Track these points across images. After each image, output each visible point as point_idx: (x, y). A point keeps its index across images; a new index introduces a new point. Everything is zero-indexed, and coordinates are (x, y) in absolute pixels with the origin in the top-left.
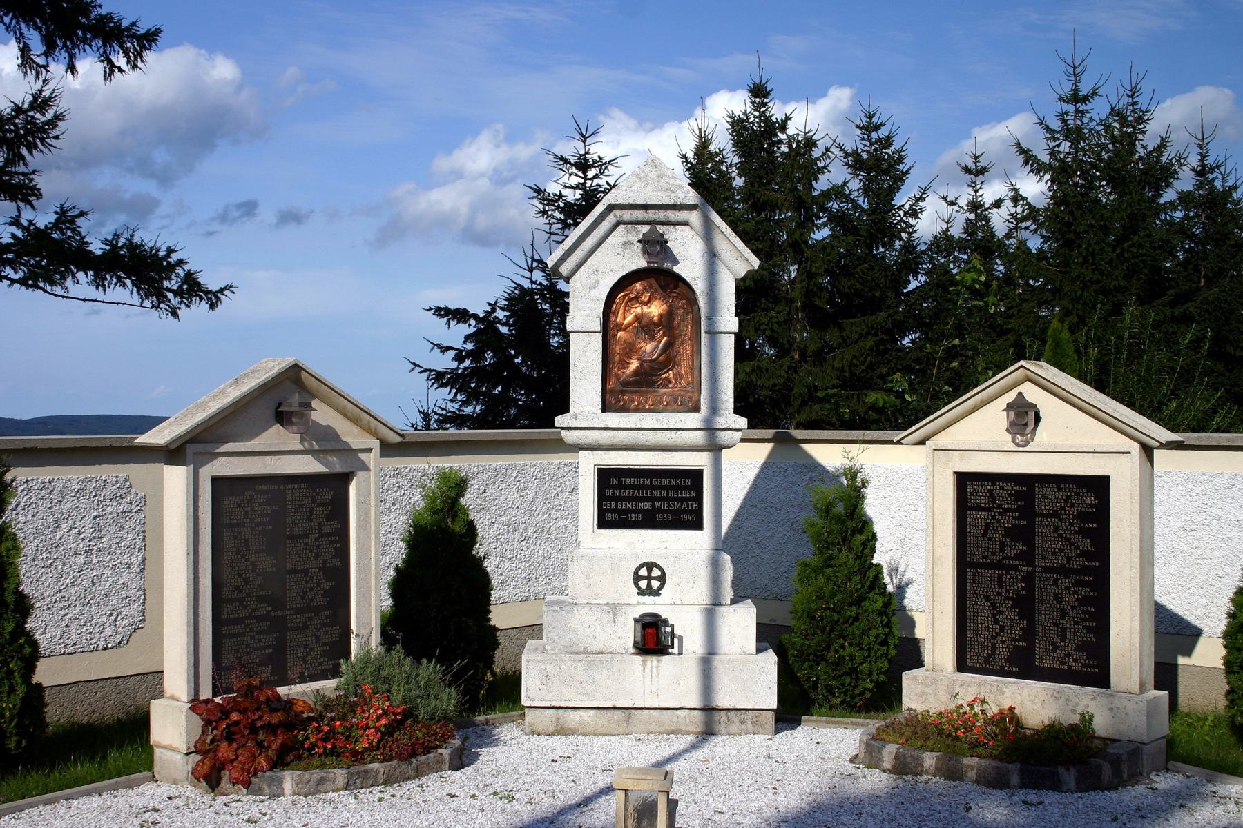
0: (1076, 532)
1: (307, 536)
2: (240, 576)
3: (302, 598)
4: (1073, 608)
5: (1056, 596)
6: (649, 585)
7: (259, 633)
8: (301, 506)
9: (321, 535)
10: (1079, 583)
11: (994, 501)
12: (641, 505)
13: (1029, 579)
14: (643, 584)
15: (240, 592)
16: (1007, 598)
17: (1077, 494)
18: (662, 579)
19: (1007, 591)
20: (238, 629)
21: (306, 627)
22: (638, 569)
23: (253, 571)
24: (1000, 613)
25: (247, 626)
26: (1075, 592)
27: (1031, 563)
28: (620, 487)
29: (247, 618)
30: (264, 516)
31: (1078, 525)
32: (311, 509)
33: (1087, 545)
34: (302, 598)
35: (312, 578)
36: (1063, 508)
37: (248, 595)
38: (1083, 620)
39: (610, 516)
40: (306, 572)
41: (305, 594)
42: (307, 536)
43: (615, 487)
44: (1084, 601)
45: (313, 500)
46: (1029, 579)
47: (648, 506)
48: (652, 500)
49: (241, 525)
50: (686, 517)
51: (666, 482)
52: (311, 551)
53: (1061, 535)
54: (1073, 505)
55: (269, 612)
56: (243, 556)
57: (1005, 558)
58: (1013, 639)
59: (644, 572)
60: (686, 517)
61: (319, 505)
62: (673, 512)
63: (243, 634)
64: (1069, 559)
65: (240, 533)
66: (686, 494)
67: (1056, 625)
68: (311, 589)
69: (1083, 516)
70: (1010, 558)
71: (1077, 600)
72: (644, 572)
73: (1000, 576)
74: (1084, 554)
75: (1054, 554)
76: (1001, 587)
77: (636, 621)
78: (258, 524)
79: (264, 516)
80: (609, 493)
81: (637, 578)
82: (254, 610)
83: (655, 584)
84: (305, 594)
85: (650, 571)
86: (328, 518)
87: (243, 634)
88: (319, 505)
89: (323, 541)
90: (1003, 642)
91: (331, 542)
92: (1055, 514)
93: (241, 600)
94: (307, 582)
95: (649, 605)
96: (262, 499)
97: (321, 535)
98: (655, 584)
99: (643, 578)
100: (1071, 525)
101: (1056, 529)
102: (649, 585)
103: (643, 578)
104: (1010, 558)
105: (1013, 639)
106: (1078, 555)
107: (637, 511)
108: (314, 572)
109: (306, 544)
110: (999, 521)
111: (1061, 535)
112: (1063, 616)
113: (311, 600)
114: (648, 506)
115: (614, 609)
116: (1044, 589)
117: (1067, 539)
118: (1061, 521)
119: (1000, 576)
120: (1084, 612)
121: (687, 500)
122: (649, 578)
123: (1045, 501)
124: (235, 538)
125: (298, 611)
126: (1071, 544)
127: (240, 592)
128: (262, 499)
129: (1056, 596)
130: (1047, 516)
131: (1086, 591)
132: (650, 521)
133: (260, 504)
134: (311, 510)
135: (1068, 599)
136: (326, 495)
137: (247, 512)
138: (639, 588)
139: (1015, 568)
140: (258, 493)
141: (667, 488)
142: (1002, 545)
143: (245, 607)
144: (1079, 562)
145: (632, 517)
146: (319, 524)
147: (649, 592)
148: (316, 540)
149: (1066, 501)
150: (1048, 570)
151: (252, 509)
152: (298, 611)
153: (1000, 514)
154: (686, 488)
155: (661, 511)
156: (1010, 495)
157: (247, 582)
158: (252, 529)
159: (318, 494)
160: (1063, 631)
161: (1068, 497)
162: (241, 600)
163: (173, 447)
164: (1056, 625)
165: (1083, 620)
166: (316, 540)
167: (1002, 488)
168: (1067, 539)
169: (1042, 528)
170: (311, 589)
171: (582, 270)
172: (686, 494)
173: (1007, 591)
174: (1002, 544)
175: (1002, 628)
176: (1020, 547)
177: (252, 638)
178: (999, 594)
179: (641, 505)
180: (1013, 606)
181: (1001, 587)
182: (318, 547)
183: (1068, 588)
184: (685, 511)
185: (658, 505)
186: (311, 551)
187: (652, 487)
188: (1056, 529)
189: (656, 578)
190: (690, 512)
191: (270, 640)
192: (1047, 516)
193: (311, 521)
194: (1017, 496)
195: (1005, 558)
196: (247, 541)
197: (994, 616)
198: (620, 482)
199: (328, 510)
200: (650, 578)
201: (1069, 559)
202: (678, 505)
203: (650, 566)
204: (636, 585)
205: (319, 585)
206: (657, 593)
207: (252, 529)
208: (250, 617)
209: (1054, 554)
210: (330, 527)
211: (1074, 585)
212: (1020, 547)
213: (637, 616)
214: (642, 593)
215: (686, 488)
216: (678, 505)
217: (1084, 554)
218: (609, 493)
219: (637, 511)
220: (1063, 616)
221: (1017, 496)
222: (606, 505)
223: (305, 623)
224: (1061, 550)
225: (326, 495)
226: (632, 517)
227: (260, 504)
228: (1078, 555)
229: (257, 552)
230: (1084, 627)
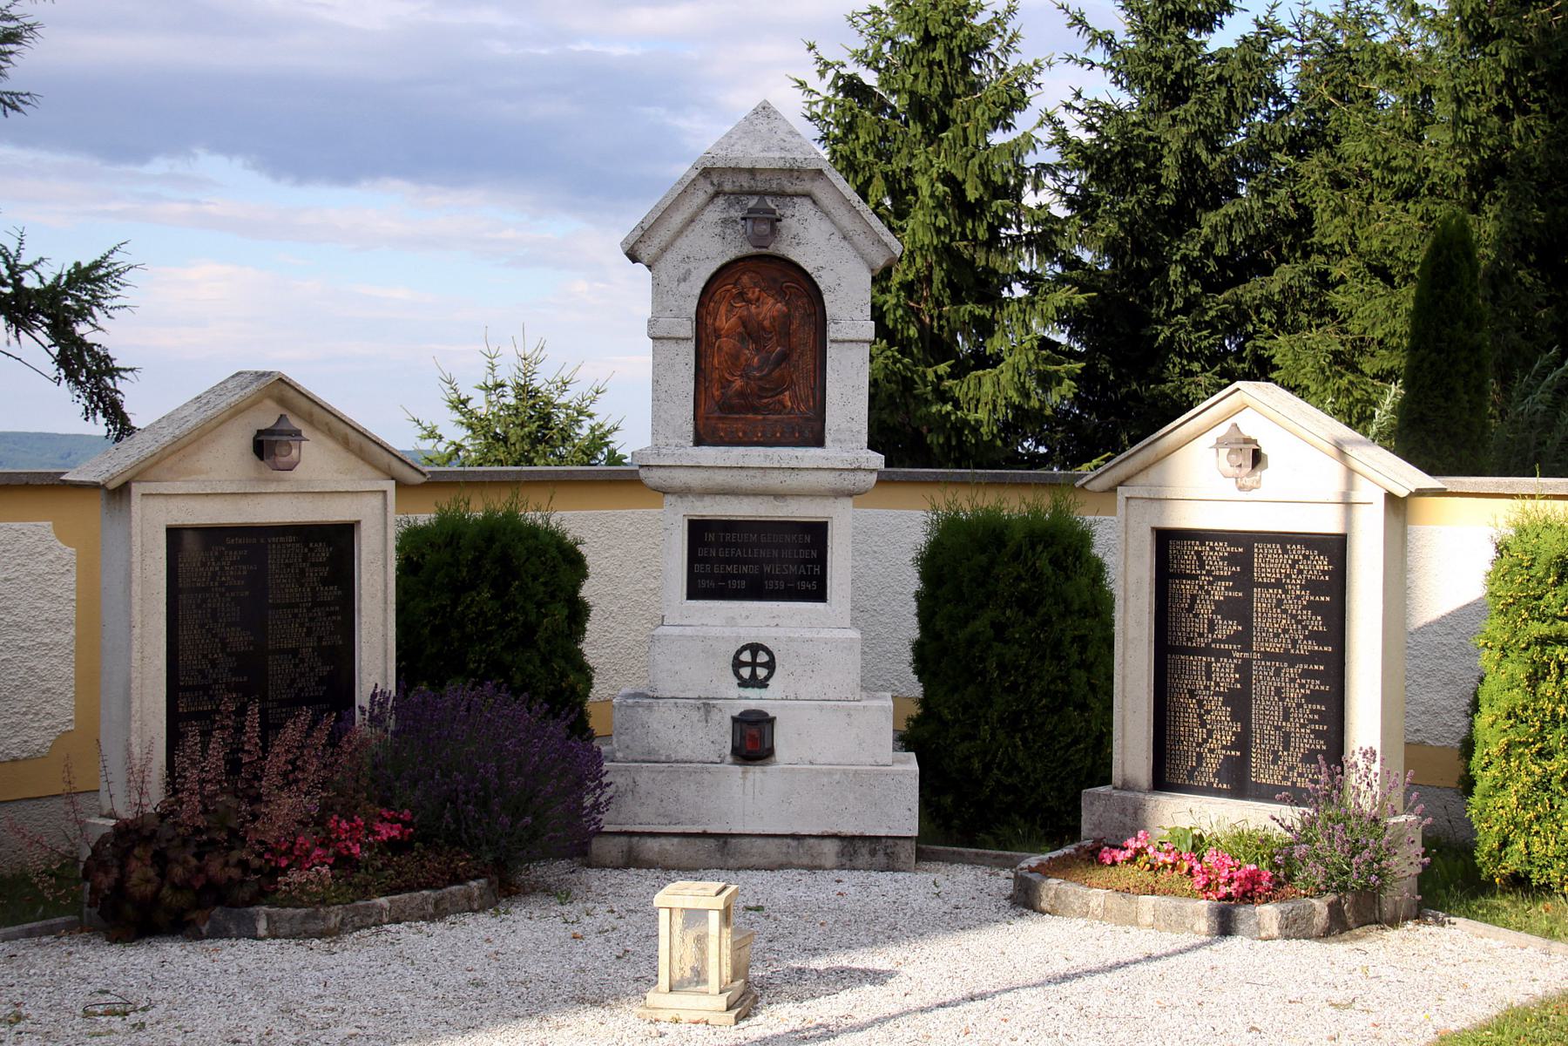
0: (1304, 607)
1: (297, 605)
3: (290, 686)
4: (1299, 706)
5: (1278, 691)
6: (754, 673)
8: (288, 566)
10: (1306, 674)
11: (1202, 567)
12: (745, 569)
13: (1244, 669)
15: (205, 677)
17: (1306, 557)
18: (771, 666)
19: (1217, 684)
22: (739, 652)
24: (1208, 712)
26: (1302, 686)
27: (1247, 647)
30: (237, 578)
31: (1307, 596)
33: (1317, 623)
36: (1288, 576)
37: (216, 681)
38: (1312, 721)
39: (703, 584)
40: (294, 652)
41: (293, 681)
42: (297, 605)
44: (1313, 697)
46: (1244, 669)
50: (803, 585)
52: (302, 625)
53: (1285, 611)
54: (1300, 572)
57: (1214, 641)
58: (1224, 747)
60: (803, 585)
61: (313, 565)
64: (1294, 642)
65: (204, 601)
67: (1278, 728)
68: (302, 675)
69: (1312, 586)
70: (1221, 641)
71: (1304, 695)
72: (746, 657)
75: (1277, 635)
76: (1209, 678)
77: (734, 720)
79: (237, 578)
80: (702, 552)
81: (737, 664)
84: (293, 681)
85: (754, 656)
86: (325, 582)
88: (313, 565)
90: (1211, 751)
92: (1279, 584)
94: (296, 666)
95: (753, 700)
99: (745, 664)
100: (1299, 597)
101: (1280, 602)
102: (754, 673)
103: (745, 664)
104: (1221, 641)
105: (1224, 747)
106: (1306, 638)
109: (295, 616)
111: (1285, 611)
112: (1286, 719)
113: (301, 690)
115: (706, 706)
116: (1263, 685)
117: (1294, 617)
118: (1286, 592)
119: (1209, 665)
120: (1313, 712)
122: (754, 664)
123: (1267, 565)
126: (1299, 622)
127: (205, 677)
129: (1278, 691)
130: (1267, 586)
131: (1315, 685)
132: (756, 590)
133: (233, 563)
135: (1293, 694)
136: (323, 553)
137: (214, 573)
139: (1228, 654)
142: (1211, 623)
144: (1306, 647)
145: (733, 584)
146: (313, 589)
147: (754, 682)
149: (1292, 567)
150: (1267, 656)
151: (222, 568)
155: (771, 577)
156: (1223, 559)
157: (214, 664)
158: (222, 595)
159: (311, 550)
160: (1287, 736)
161: (1295, 562)
164: (1278, 728)
165: (1312, 721)
166: (309, 610)
167: (1212, 549)
168: (1294, 617)
169: (1262, 600)
171: (669, 256)
173: (1217, 684)
174: (1211, 622)
175: (1210, 733)
176: (1234, 627)
179: (745, 569)
180: (1224, 704)
181: (1209, 678)
182: (311, 619)
183: (1293, 680)
185: (767, 569)
186: (302, 625)
188: (1280, 602)
189: (762, 665)
190: (809, 578)
192: (1267, 586)
193: (302, 585)
194: (1232, 559)
195: (1214, 641)
197: (1200, 716)
199: (325, 572)
200: (754, 664)
201: (1294, 642)
203: (755, 648)
204: (737, 674)
205: (312, 669)
206: (763, 684)
209: (1277, 635)
210: (331, 592)
212: (1234, 627)
213: (736, 713)
214: (743, 683)
218: (702, 552)
220: (1286, 719)
221: (1232, 559)
222: (698, 568)
224: (1285, 631)
226: (733, 584)
227: (233, 563)
228: (1306, 638)
230: (1313, 731)
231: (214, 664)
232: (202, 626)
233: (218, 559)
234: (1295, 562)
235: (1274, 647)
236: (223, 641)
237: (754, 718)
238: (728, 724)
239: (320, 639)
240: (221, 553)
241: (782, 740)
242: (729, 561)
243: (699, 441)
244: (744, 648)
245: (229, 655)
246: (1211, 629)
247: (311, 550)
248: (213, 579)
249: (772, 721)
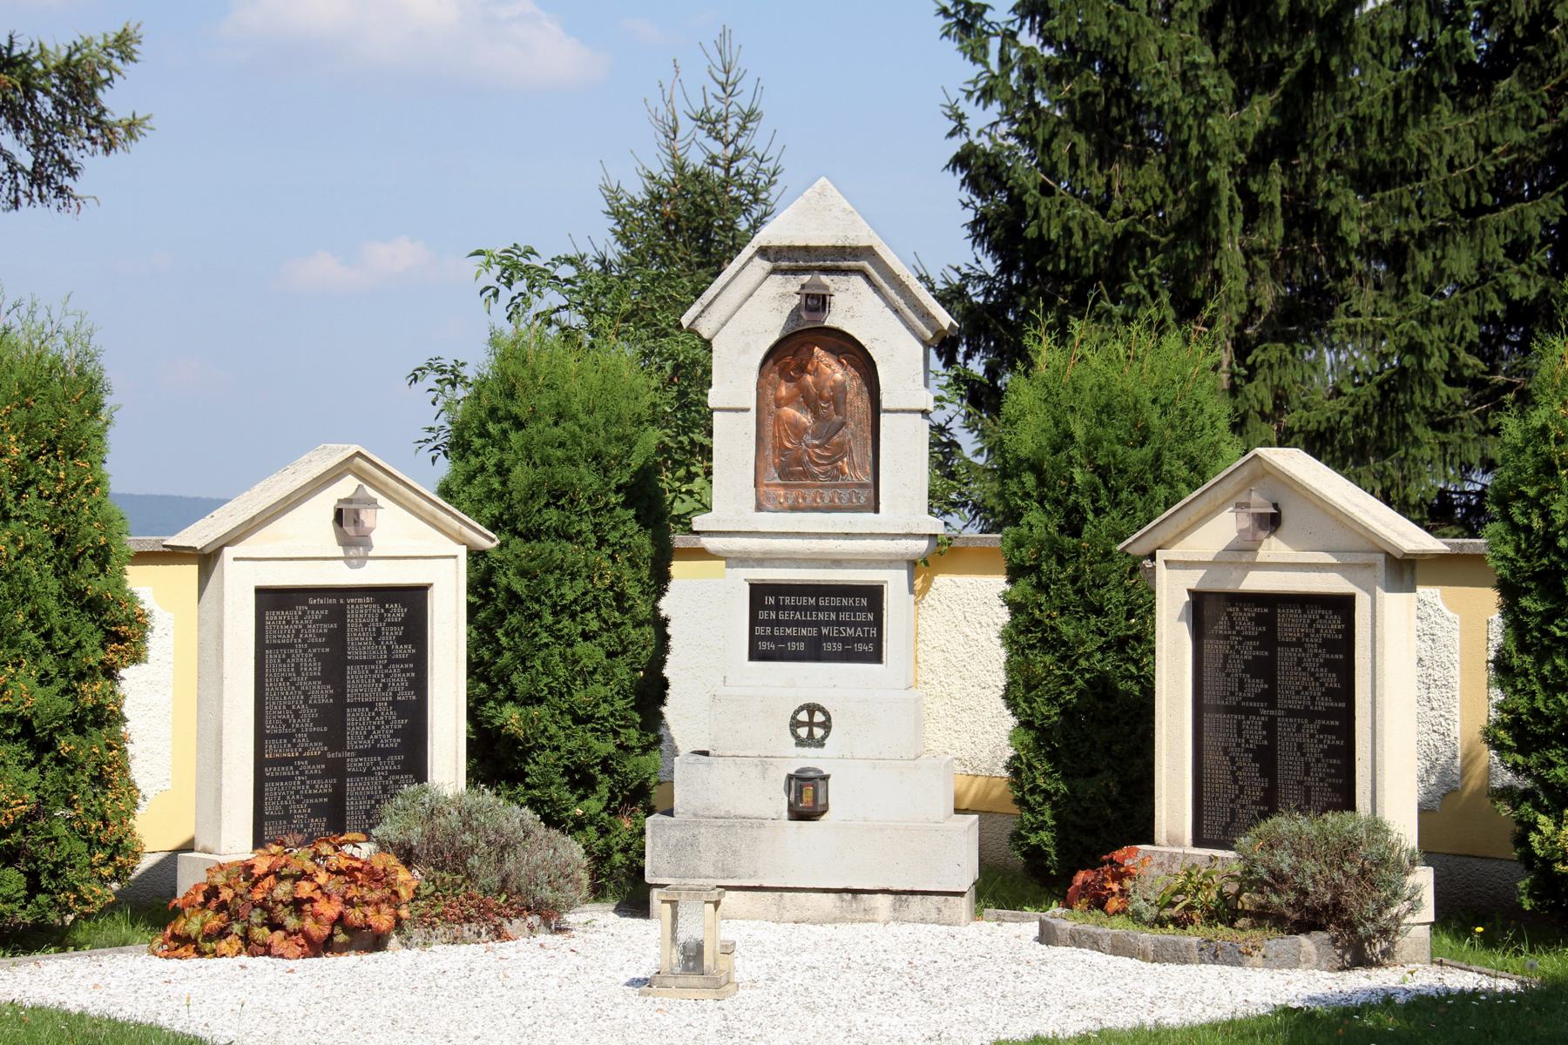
0: (1321, 665)
1: (373, 662)
2: (289, 707)
3: (367, 737)
4: (1318, 760)
5: (1300, 746)
6: (811, 733)
7: (311, 777)
8: (365, 625)
9: (391, 661)
10: (1324, 730)
11: (1233, 628)
13: (1270, 726)
14: (803, 732)
15: (289, 726)
16: (1247, 750)
17: (1322, 617)
18: (826, 726)
19: (1247, 741)
20: (286, 771)
21: (370, 773)
22: (797, 712)
23: (305, 702)
24: (1239, 769)
25: (296, 768)
26: (1320, 741)
27: (1272, 705)
28: (777, 607)
29: (296, 759)
30: (319, 635)
32: (379, 629)
33: (1332, 680)
34: (367, 737)
35: (378, 714)
36: (1307, 635)
37: (299, 731)
38: (1330, 775)
39: (763, 646)
40: (371, 705)
41: (370, 732)
42: (373, 662)
43: (769, 608)
44: (1331, 752)
45: (381, 618)
46: (1270, 726)
47: (814, 632)
48: (817, 624)
49: (292, 646)
50: (860, 647)
51: (836, 601)
52: (378, 681)
53: (1304, 669)
54: (1317, 631)
55: (324, 753)
56: (293, 684)
57: (1245, 699)
58: (1254, 803)
59: (803, 716)
60: (860, 647)
61: (389, 624)
62: (845, 641)
63: (292, 778)
64: (1313, 699)
65: (289, 656)
66: (861, 617)
67: (1300, 783)
68: (378, 727)
69: (1328, 645)
70: (1250, 699)
71: (1323, 751)
72: (803, 716)
73: (1240, 722)
74: (1329, 693)
75: (1298, 693)
76: (1240, 736)
78: (312, 646)
79: (319, 635)
80: (763, 615)
81: (795, 724)
82: (305, 749)
83: (818, 732)
84: (370, 732)
85: (811, 715)
86: (400, 640)
87: (292, 778)
88: (389, 624)
89: (396, 668)
90: (1243, 807)
91: (404, 671)
92: (1299, 643)
93: (290, 737)
94: (372, 718)
95: (809, 758)
96: (318, 615)
97: (391, 661)
98: (818, 732)
99: (802, 724)
100: (1316, 655)
101: (1300, 661)
102: (811, 733)
103: (802, 724)
104: (1250, 699)
105: (1254, 803)
106: (1324, 694)
107: (797, 639)
108: (381, 707)
109: (372, 672)
110: (1238, 652)
111: (1304, 669)
112: (1307, 774)
113: (377, 741)
114: (814, 632)
115: (764, 761)
117: (1312, 674)
118: (1305, 651)
120: (1330, 766)
121: (862, 624)
122: (811, 724)
123: (1290, 624)
124: (283, 661)
125: (361, 753)
126: (1317, 679)
127: (289, 726)
128: (318, 615)
129: (1300, 746)
130: (1289, 645)
131: (1331, 740)
132: (814, 652)
133: (315, 622)
134: (379, 629)
135: (1314, 749)
136: (398, 612)
137: (298, 631)
138: (797, 737)
139: (1256, 712)
140: (312, 607)
141: (838, 610)
143: (294, 745)
144: (1323, 703)
145: (792, 646)
146: (389, 647)
147: (810, 742)
148: (385, 667)
149: (1310, 626)
150: (1291, 713)
151: (305, 626)
152: (361, 753)
153: (1240, 643)
154: (861, 609)
155: (829, 639)
156: (1251, 619)
157: (297, 714)
158: (305, 651)
159: (387, 611)
160: (1308, 789)
161: (1313, 621)
162: (290, 737)
163: (208, 551)
164: (1300, 783)
165: (1330, 775)
166: (385, 667)
168: (1312, 674)
170: (378, 727)
172: (861, 617)
173: (1247, 741)
174: (1241, 681)
175: (1241, 789)
176: (1262, 685)
177: (303, 783)
178: (1239, 745)
179: (804, 632)
180: (1254, 760)
182: (387, 676)
183: (1312, 736)
184: (859, 640)
185: (825, 631)
186: (378, 681)
187: (818, 608)
188: (1300, 661)
189: (819, 725)
190: (866, 641)
191: (325, 787)
192: (1289, 645)
193: (378, 643)
194: (1258, 619)
195: (1245, 699)
196: (297, 665)
197: (1233, 773)
198: (777, 601)
199: (399, 631)
200: (811, 724)
201: (1313, 699)
202: (850, 632)
203: (811, 709)
204: (794, 733)
205: (387, 722)
207: (305, 651)
208: (301, 758)
209: (1298, 693)
210: (407, 650)
211: (1320, 732)
212: (1262, 685)
213: (792, 772)
214: (800, 742)
215: (861, 609)
216: (850, 632)
217: (1329, 693)
218: (763, 615)
219: (797, 639)
220: (1307, 774)
221: (1258, 619)
222: (759, 630)
223: (369, 769)
224: (1305, 688)
225: (398, 612)
226: (792, 646)
227: (315, 622)
228: (1324, 694)
229: (311, 679)
230: (1331, 785)
231: (297, 714)
232: (286, 679)
233: (301, 618)
234: (1313, 621)
235: (1295, 703)
236: (305, 693)
237: (811, 774)
238: (784, 778)
239: (395, 694)
240: (304, 613)
241: (836, 794)
242: (788, 624)
243: (759, 508)
244: (802, 708)
245: (311, 706)
246: (1241, 689)
247: (387, 611)
248: (297, 636)
249: (826, 778)
